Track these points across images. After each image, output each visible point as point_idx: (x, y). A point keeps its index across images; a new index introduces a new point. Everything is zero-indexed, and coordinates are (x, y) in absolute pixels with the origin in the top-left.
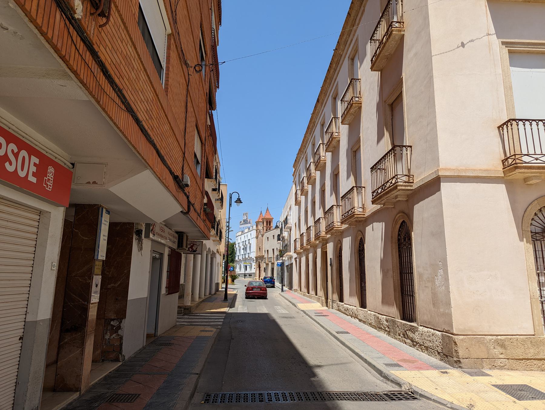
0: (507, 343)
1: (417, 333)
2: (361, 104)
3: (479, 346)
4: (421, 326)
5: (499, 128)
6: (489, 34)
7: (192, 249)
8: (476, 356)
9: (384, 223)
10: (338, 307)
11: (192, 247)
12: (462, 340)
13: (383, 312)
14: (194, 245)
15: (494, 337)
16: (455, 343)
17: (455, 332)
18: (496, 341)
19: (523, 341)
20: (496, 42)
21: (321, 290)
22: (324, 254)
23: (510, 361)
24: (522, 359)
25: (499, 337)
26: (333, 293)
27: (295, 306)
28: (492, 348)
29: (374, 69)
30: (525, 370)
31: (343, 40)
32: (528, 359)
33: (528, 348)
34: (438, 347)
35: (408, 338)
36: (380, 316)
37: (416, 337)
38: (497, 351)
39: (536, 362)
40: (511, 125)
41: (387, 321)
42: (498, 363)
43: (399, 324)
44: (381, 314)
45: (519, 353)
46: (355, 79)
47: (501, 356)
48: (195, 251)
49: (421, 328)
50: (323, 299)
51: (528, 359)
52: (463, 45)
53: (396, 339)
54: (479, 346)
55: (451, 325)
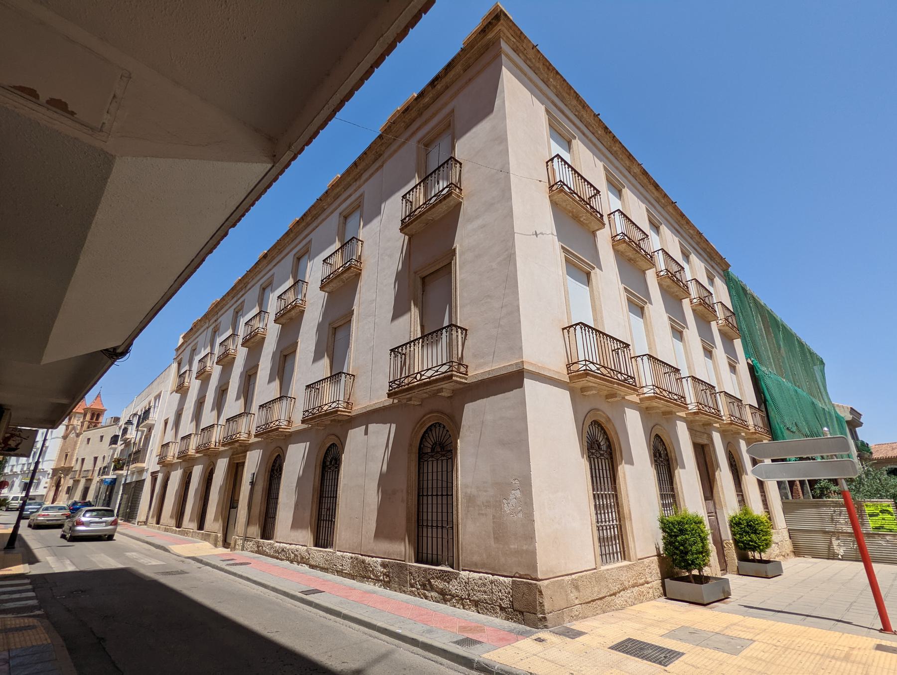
0: (580, 583)
1: (454, 582)
2: (361, 270)
3: (560, 592)
4: (463, 570)
9: (394, 426)
10: (258, 547)
13: (374, 553)
16: (540, 592)
17: (540, 577)
21: (216, 519)
22: (236, 470)
25: (573, 576)
26: (249, 523)
27: (166, 550)
31: (335, 191)
34: (501, 599)
35: (432, 588)
36: (367, 559)
37: (454, 587)
41: (384, 565)
43: (413, 570)
44: (369, 556)
46: (357, 239)
49: (461, 572)
50: (219, 535)
52: (536, 234)
53: (405, 592)
54: (560, 592)
55: (534, 567)
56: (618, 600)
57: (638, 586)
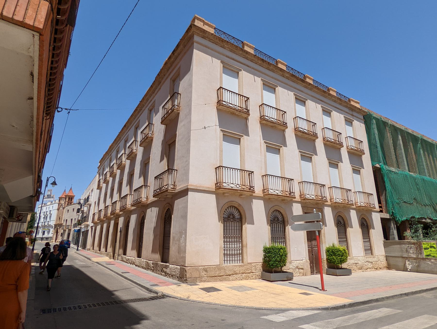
0: (208, 269)
1: (168, 269)
2: (153, 138)
3: (196, 272)
4: (171, 264)
5: (216, 168)
7: (18, 219)
8: (194, 277)
10: (122, 258)
11: (18, 217)
12: (189, 269)
13: (151, 259)
14: (20, 215)
15: (203, 267)
16: (186, 271)
17: (186, 266)
18: (204, 269)
19: (215, 268)
20: (218, 129)
21: (110, 247)
22: (116, 225)
23: (209, 278)
24: (213, 277)
25: (205, 267)
26: (119, 248)
27: (90, 260)
28: (202, 272)
29: (162, 123)
30: (214, 281)
32: (216, 276)
33: (217, 271)
34: (178, 274)
35: (163, 272)
36: (149, 261)
37: (168, 271)
38: (203, 273)
39: (218, 277)
40: (220, 168)
41: (153, 264)
42: (203, 279)
43: (159, 265)
44: (150, 261)
45: (212, 274)
47: (205, 276)
48: (21, 220)
49: (171, 265)
50: (111, 254)
51: (216, 276)
52: (205, 128)
53: (157, 273)
54: (196, 272)
55: (185, 262)
56: (231, 278)
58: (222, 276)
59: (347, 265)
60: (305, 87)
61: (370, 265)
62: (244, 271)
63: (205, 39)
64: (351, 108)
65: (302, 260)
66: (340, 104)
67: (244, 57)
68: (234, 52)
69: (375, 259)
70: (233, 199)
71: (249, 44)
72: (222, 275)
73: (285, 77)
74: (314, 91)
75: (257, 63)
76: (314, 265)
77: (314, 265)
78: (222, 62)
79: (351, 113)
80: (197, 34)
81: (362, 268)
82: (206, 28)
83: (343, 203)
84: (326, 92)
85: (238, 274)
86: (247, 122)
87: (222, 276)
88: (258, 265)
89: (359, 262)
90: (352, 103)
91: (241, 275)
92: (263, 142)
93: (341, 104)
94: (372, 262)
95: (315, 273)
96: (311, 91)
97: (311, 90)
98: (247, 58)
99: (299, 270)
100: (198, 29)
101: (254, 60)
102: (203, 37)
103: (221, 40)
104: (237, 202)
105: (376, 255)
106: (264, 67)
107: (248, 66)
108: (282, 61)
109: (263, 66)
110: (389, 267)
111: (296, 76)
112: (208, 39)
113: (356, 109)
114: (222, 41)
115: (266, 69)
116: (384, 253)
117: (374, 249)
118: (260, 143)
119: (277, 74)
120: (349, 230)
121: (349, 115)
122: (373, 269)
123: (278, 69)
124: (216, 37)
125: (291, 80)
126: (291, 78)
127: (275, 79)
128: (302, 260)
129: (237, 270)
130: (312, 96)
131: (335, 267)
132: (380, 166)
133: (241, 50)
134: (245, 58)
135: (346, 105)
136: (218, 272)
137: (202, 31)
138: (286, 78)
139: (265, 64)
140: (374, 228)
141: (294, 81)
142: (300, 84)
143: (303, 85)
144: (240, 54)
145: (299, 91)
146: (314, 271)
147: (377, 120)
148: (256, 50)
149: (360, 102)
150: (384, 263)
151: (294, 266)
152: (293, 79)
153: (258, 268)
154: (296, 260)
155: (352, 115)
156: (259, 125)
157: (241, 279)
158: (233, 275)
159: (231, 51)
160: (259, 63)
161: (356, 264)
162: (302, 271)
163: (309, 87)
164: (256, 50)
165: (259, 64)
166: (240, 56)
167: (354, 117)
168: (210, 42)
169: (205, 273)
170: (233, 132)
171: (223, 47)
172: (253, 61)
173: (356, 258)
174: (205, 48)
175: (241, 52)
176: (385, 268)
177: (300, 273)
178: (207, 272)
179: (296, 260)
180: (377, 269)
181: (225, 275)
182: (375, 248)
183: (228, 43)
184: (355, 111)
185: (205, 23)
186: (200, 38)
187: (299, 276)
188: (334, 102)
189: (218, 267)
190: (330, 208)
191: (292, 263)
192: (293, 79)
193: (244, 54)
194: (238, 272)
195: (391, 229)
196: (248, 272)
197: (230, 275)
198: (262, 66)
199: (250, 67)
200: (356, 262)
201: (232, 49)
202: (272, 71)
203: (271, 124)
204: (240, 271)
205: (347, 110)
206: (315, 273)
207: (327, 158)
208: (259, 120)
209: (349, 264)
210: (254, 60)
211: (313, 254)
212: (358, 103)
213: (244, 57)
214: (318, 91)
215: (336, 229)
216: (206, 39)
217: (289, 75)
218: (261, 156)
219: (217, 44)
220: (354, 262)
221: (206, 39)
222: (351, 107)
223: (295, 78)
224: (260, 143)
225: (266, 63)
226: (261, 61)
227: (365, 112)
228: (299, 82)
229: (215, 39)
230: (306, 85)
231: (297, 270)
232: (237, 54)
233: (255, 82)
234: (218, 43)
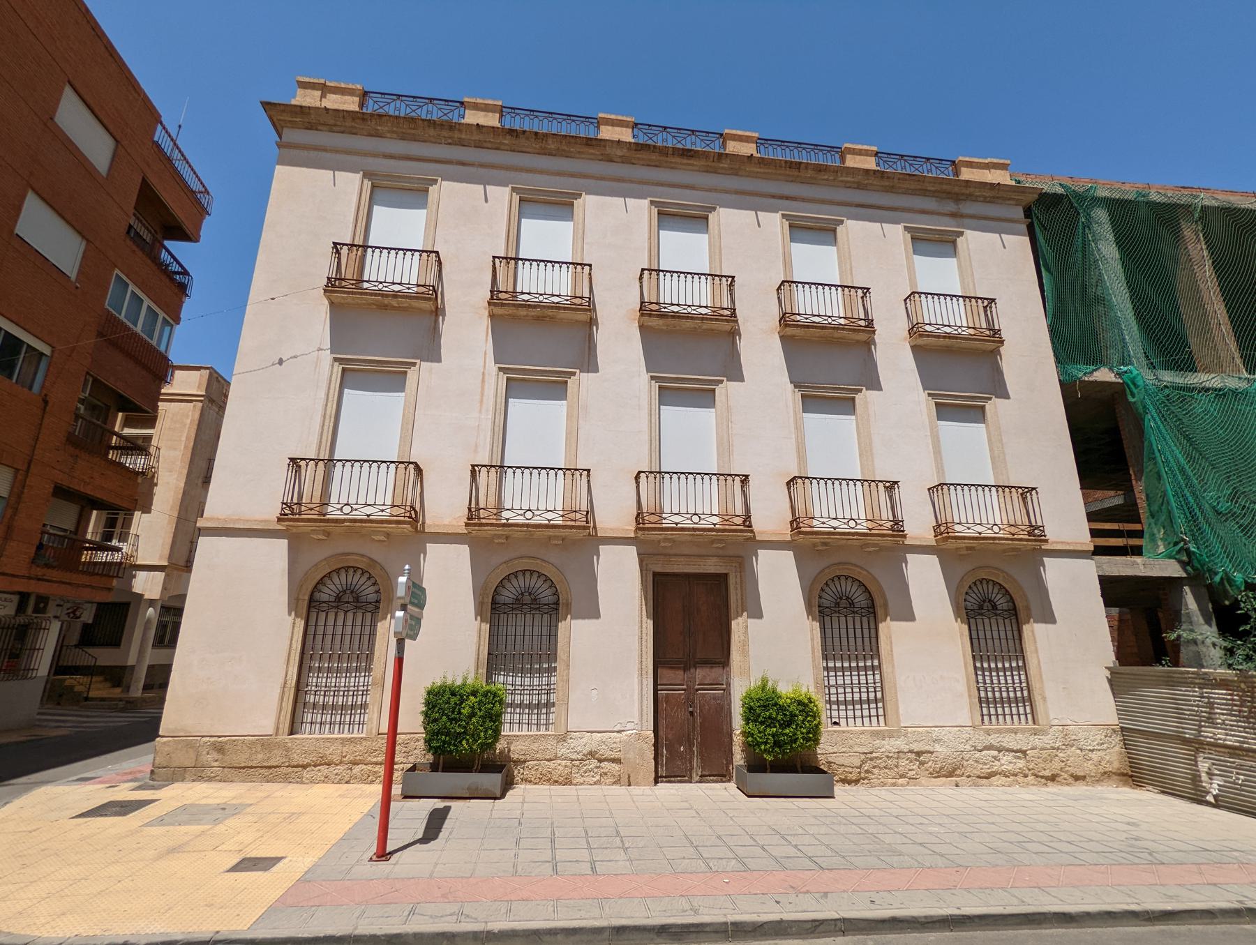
0: (227, 747)
6: (320, 349)
8: (179, 765)
12: (165, 743)
15: (212, 739)
18: (213, 744)
19: (253, 743)
23: (226, 770)
24: (244, 768)
28: (204, 753)
30: (243, 781)
32: (252, 767)
33: (257, 752)
38: (210, 758)
39: (261, 771)
42: (208, 772)
45: (242, 759)
47: (216, 764)
51: (252, 767)
57: (366, 764)
58: (275, 767)
59: (863, 757)
60: (707, 172)
61: (1006, 762)
62: (358, 758)
63: (317, 130)
64: (949, 193)
65: (619, 732)
66: (891, 190)
67: (450, 144)
68: (415, 139)
69: (1047, 740)
70: (352, 546)
71: (479, 101)
72: (274, 764)
73: (619, 160)
74: (750, 175)
75: (502, 147)
76: (695, 749)
77: (695, 749)
78: (367, 175)
79: (950, 207)
80: (288, 125)
81: (958, 772)
82: (333, 102)
83: (873, 532)
84: (802, 166)
85: (337, 765)
86: (436, 321)
87: (275, 767)
88: (418, 740)
89: (937, 748)
90: (966, 174)
91: (346, 767)
92: (492, 368)
93: (893, 187)
94: (1024, 752)
95: (696, 778)
96: (736, 177)
97: (737, 175)
98: (461, 143)
99: (602, 765)
100: (283, 111)
101: (485, 142)
102: (311, 127)
103: (358, 118)
104: (363, 556)
105: (1055, 722)
106: (528, 150)
107: (463, 164)
108: (613, 117)
109: (524, 149)
110: (1134, 775)
111: (655, 147)
112: (325, 129)
113: (972, 190)
114: (363, 119)
115: (539, 154)
116: (1112, 718)
117: (1044, 699)
118: (483, 373)
119: (583, 158)
120: (889, 627)
121: (940, 218)
122: (1031, 778)
123: (576, 143)
124: (341, 115)
125: (641, 163)
126: (638, 158)
127: (572, 175)
128: (619, 732)
129: (333, 752)
130: (737, 192)
131: (796, 766)
132: (1120, 375)
133: (429, 126)
134: (456, 144)
135: (913, 186)
136: (260, 756)
137: (296, 113)
138: (623, 162)
139: (522, 141)
140: (1049, 618)
141: (657, 163)
142: (684, 167)
143: (696, 168)
144: (433, 136)
145: (677, 191)
146: (692, 769)
147: (1120, 210)
148: (501, 111)
149: (1009, 162)
150: (1113, 755)
151: (579, 749)
152: (644, 156)
153: (416, 751)
154: (592, 732)
155: (954, 215)
156: (484, 324)
157: (346, 779)
158: (315, 766)
159: (403, 137)
160: (507, 145)
161: (919, 754)
162: (615, 767)
163: (723, 168)
164: (501, 111)
165: (506, 147)
166: (435, 143)
167: (966, 221)
168: (334, 132)
169: (215, 755)
170: (377, 358)
171: (377, 135)
172: (485, 145)
173: (919, 733)
174: (313, 154)
175: (432, 132)
176: (1115, 777)
177: (606, 774)
178: (223, 754)
179: (592, 732)
180: (1053, 778)
181: (287, 764)
182: (1048, 694)
183: (384, 118)
184: (970, 197)
185: (325, 89)
186: (302, 130)
187: (595, 783)
188: (858, 188)
189: (264, 743)
190: (792, 552)
191: (569, 741)
192: (644, 156)
193: (445, 133)
194: (336, 759)
195: (1183, 620)
196: (375, 760)
197: (304, 767)
198: (520, 149)
199: (472, 165)
200: (916, 747)
201: (403, 133)
202: (562, 156)
203: (532, 313)
204: (345, 756)
205: (930, 204)
206: (696, 778)
207: (791, 382)
208: (485, 309)
209: (874, 755)
210: (485, 142)
211: (691, 713)
212: (1003, 167)
213: (450, 141)
214: (770, 171)
215: (817, 625)
216: (319, 128)
217: (625, 151)
218: (480, 412)
219: (354, 131)
220: (905, 748)
221: (320, 130)
222: (945, 187)
223: (653, 152)
224: (483, 373)
225: (527, 139)
226: (508, 137)
227: (1023, 192)
228: (676, 163)
229: (341, 119)
230: (710, 164)
231: (594, 763)
232: (424, 141)
233: (486, 201)
234: (356, 128)
